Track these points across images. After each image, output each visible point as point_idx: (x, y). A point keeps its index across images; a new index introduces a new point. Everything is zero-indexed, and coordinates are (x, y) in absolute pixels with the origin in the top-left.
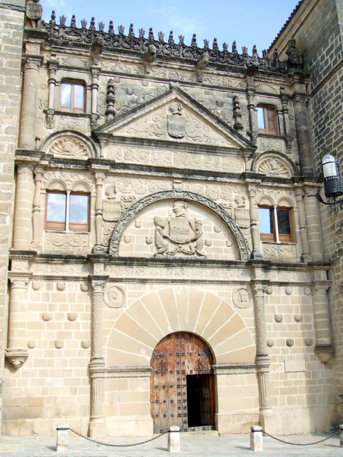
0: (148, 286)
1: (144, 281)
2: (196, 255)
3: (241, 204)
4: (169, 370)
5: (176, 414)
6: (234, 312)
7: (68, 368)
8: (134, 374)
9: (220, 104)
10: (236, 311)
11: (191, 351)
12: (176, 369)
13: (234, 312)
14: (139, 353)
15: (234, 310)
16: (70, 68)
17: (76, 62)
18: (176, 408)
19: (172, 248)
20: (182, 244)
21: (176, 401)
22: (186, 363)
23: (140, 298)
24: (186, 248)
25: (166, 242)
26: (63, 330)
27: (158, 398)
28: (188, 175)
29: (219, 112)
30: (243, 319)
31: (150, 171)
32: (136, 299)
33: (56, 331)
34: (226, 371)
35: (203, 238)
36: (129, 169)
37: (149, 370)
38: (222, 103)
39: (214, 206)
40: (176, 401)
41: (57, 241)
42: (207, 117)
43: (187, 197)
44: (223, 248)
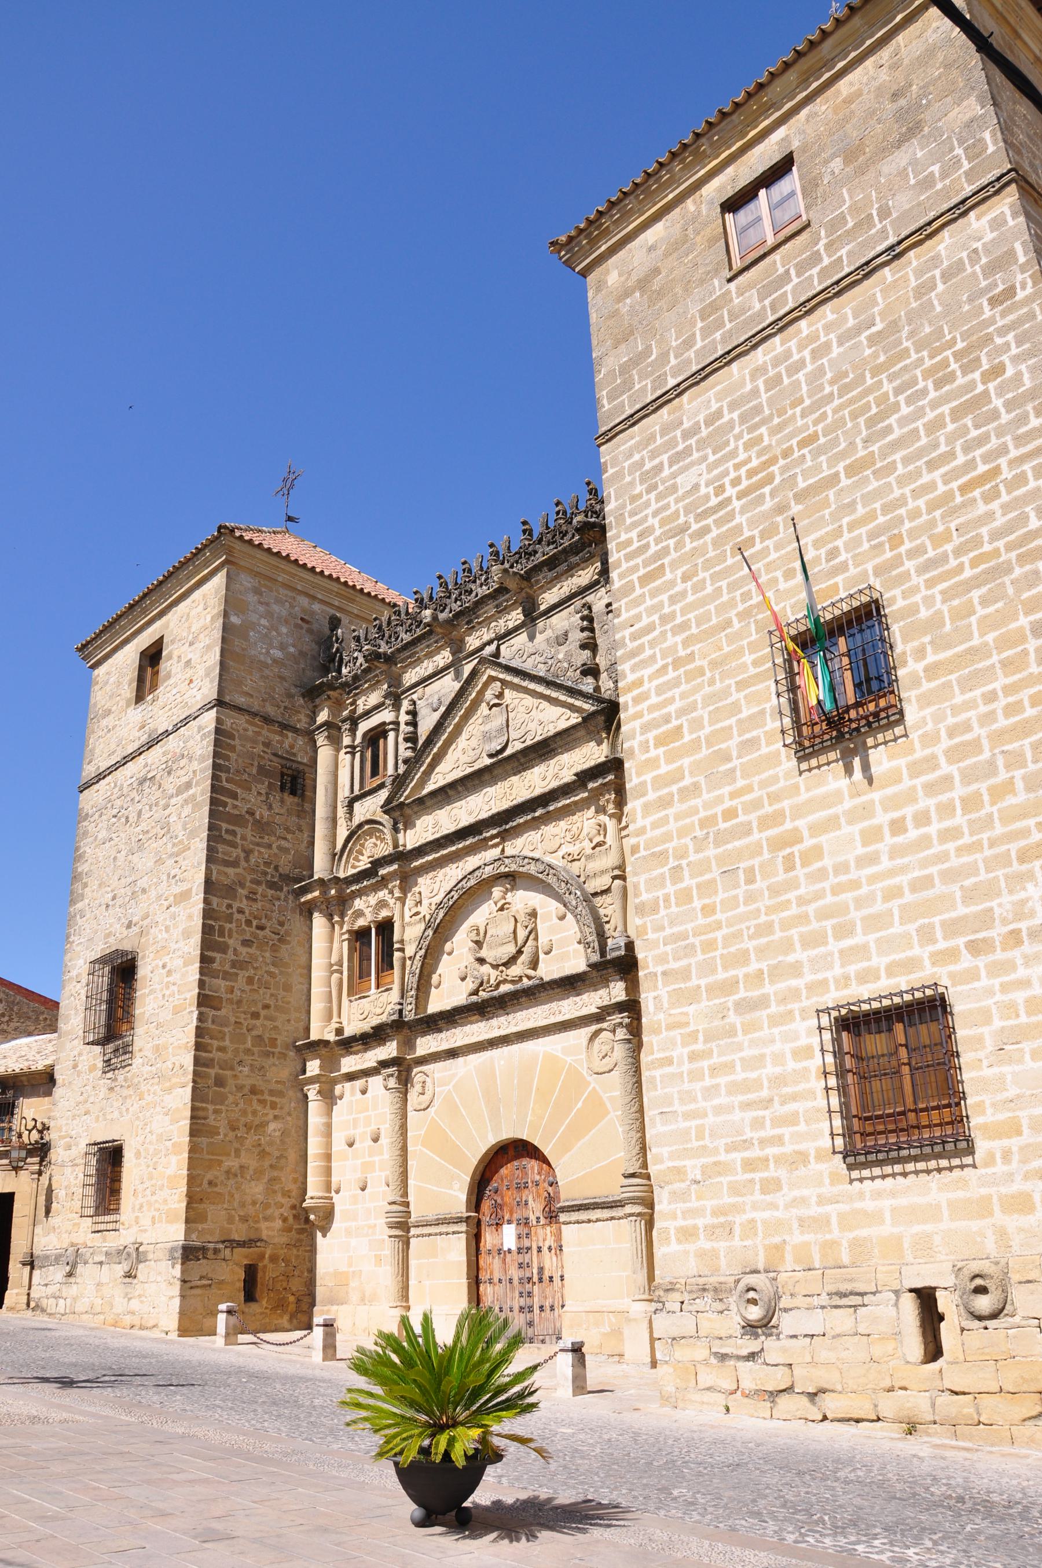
0: (461, 1060)
1: (452, 1053)
2: (525, 980)
3: (601, 838)
4: (506, 1218)
5: (516, 1309)
6: (589, 1083)
7: (372, 1222)
8: (443, 1229)
9: (561, 640)
10: (594, 1082)
11: (537, 1178)
12: (515, 1216)
13: (589, 1083)
14: (451, 1188)
15: (589, 1079)
16: (367, 714)
17: (374, 698)
18: (517, 1294)
19: (494, 974)
20: (504, 965)
21: (516, 1281)
22: (530, 1202)
23: (450, 1087)
24: (515, 971)
25: (486, 969)
26: (368, 1159)
27: (491, 1273)
28: (505, 823)
29: (561, 656)
30: (605, 1096)
31: (453, 843)
32: (446, 1088)
33: (359, 1161)
34: (575, 1216)
35: (543, 941)
36: (426, 854)
37: (459, 1220)
38: (566, 634)
39: (542, 868)
40: (516, 1281)
41: (380, 1011)
42: (532, 686)
43: (503, 869)
44: (571, 948)
